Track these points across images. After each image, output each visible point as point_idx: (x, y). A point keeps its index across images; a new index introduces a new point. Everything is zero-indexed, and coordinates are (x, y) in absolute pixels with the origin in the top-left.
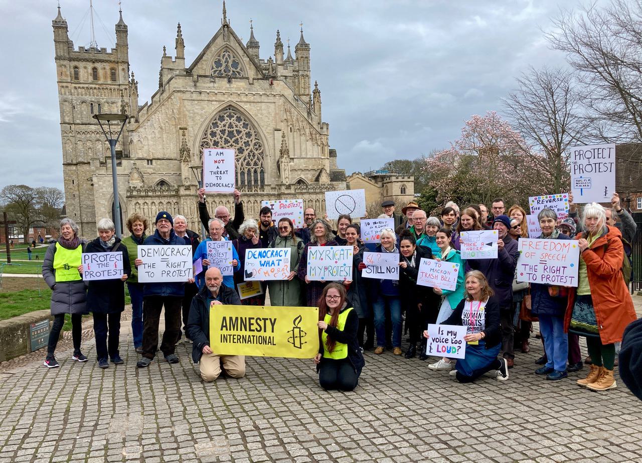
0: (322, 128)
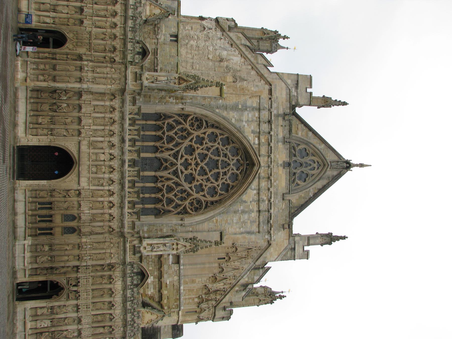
0: (224, 308)
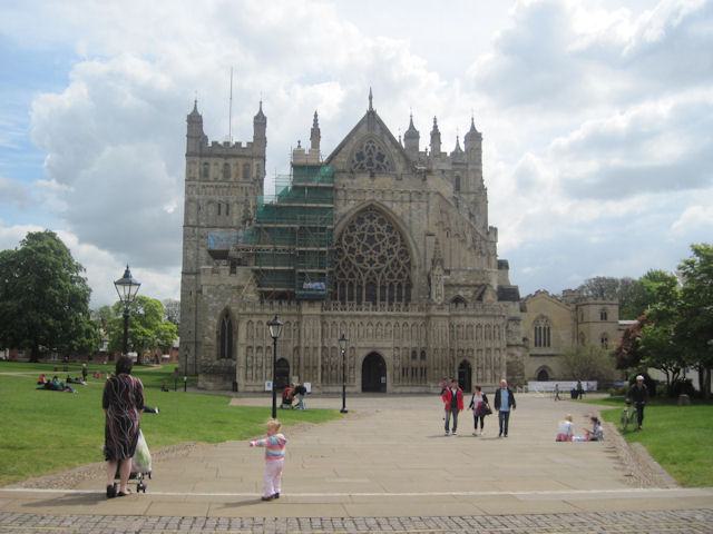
0: (488, 233)
